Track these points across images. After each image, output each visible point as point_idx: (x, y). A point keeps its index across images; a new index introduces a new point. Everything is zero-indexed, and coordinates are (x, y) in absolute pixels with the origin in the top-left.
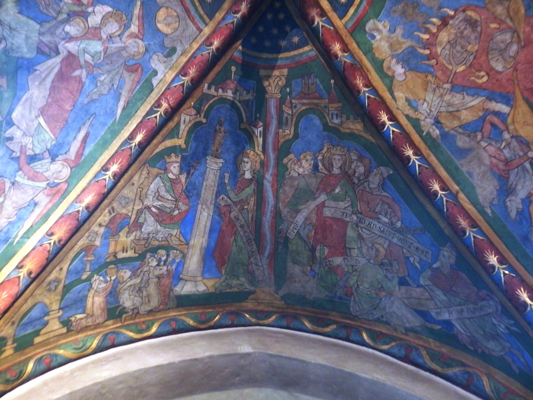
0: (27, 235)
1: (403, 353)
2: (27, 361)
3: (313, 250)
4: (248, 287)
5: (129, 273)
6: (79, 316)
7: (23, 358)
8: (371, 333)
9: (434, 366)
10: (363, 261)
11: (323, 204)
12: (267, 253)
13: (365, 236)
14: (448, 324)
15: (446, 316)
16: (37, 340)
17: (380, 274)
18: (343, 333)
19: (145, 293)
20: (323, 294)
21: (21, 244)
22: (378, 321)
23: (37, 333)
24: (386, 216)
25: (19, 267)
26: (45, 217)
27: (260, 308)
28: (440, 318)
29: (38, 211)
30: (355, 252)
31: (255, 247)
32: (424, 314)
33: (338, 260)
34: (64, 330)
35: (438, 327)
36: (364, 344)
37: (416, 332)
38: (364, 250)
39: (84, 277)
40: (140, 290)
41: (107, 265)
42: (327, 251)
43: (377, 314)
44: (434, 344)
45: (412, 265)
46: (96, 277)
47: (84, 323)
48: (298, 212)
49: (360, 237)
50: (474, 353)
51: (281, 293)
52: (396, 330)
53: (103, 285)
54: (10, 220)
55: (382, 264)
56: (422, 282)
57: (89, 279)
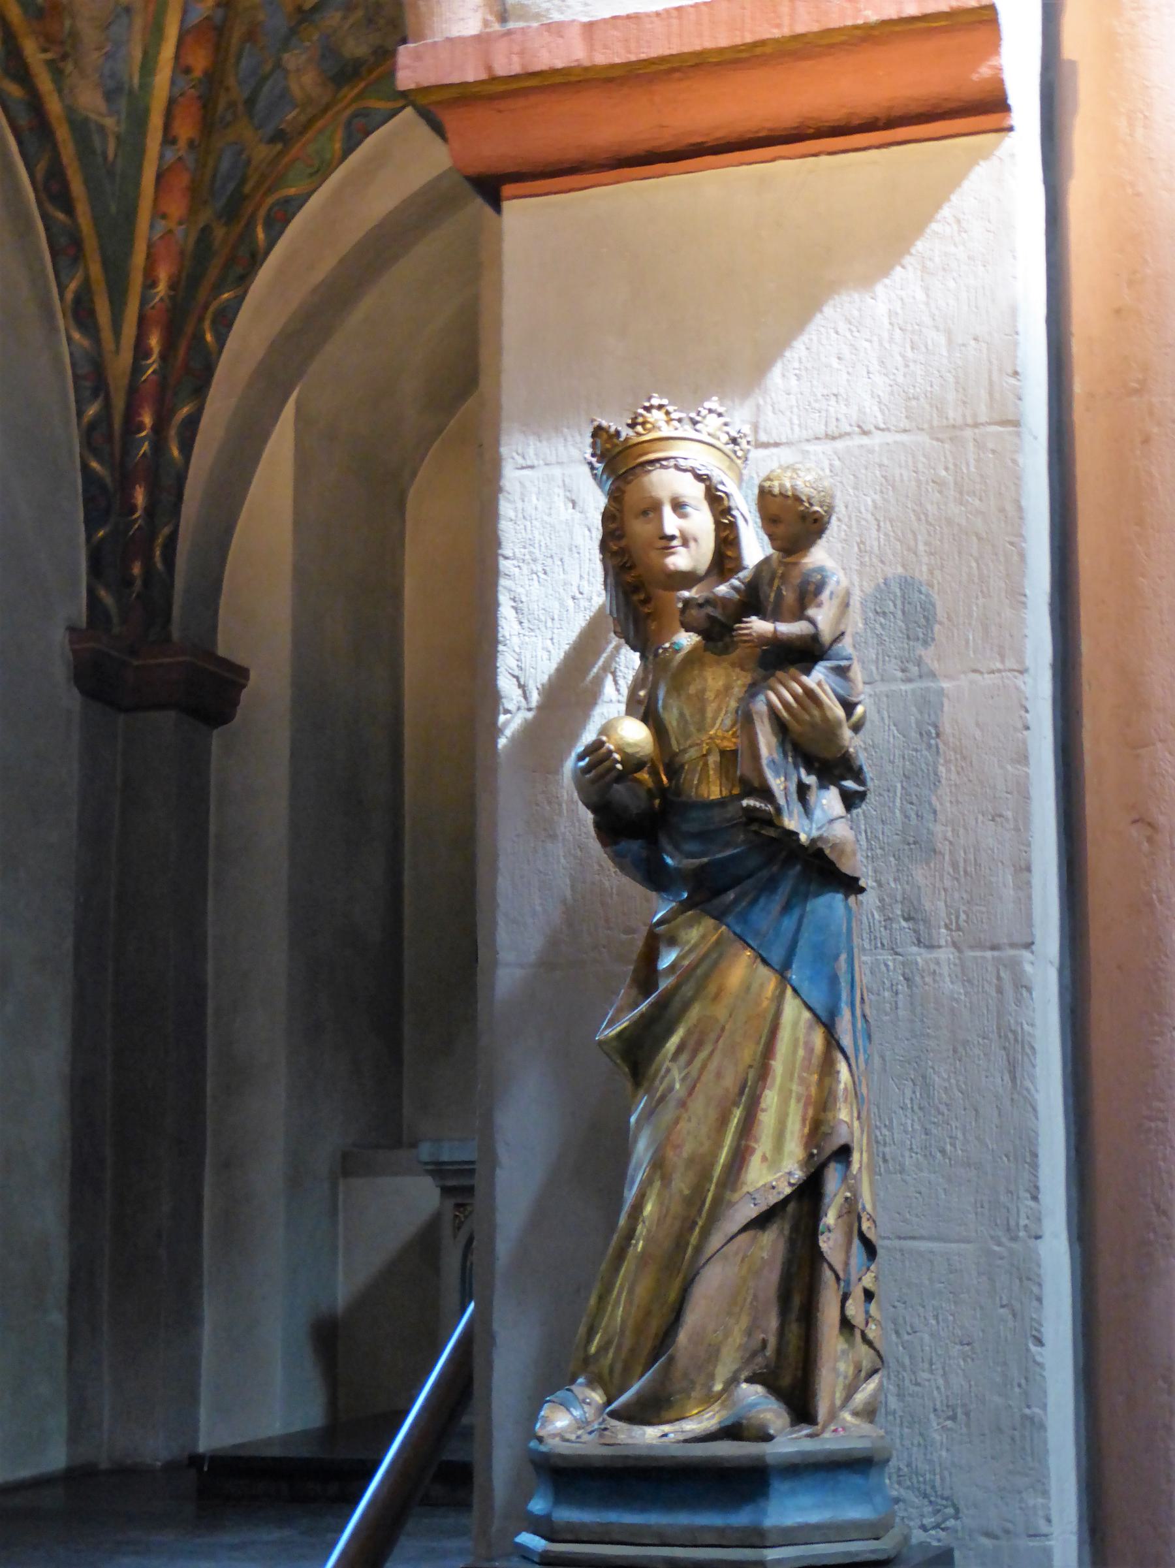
0: (148, 66)
2: (250, 225)
5: (338, 15)
6: (290, 117)
7: (242, 223)
16: (247, 189)
19: (382, 22)
21: (146, 86)
23: (243, 181)
25: (169, 139)
26: (156, 31)
29: (138, 22)
34: (279, 146)
39: (268, 67)
40: (370, 21)
41: (293, 31)
46: (286, 56)
47: (303, 118)
53: (304, 57)
54: (104, 51)
57: (278, 65)
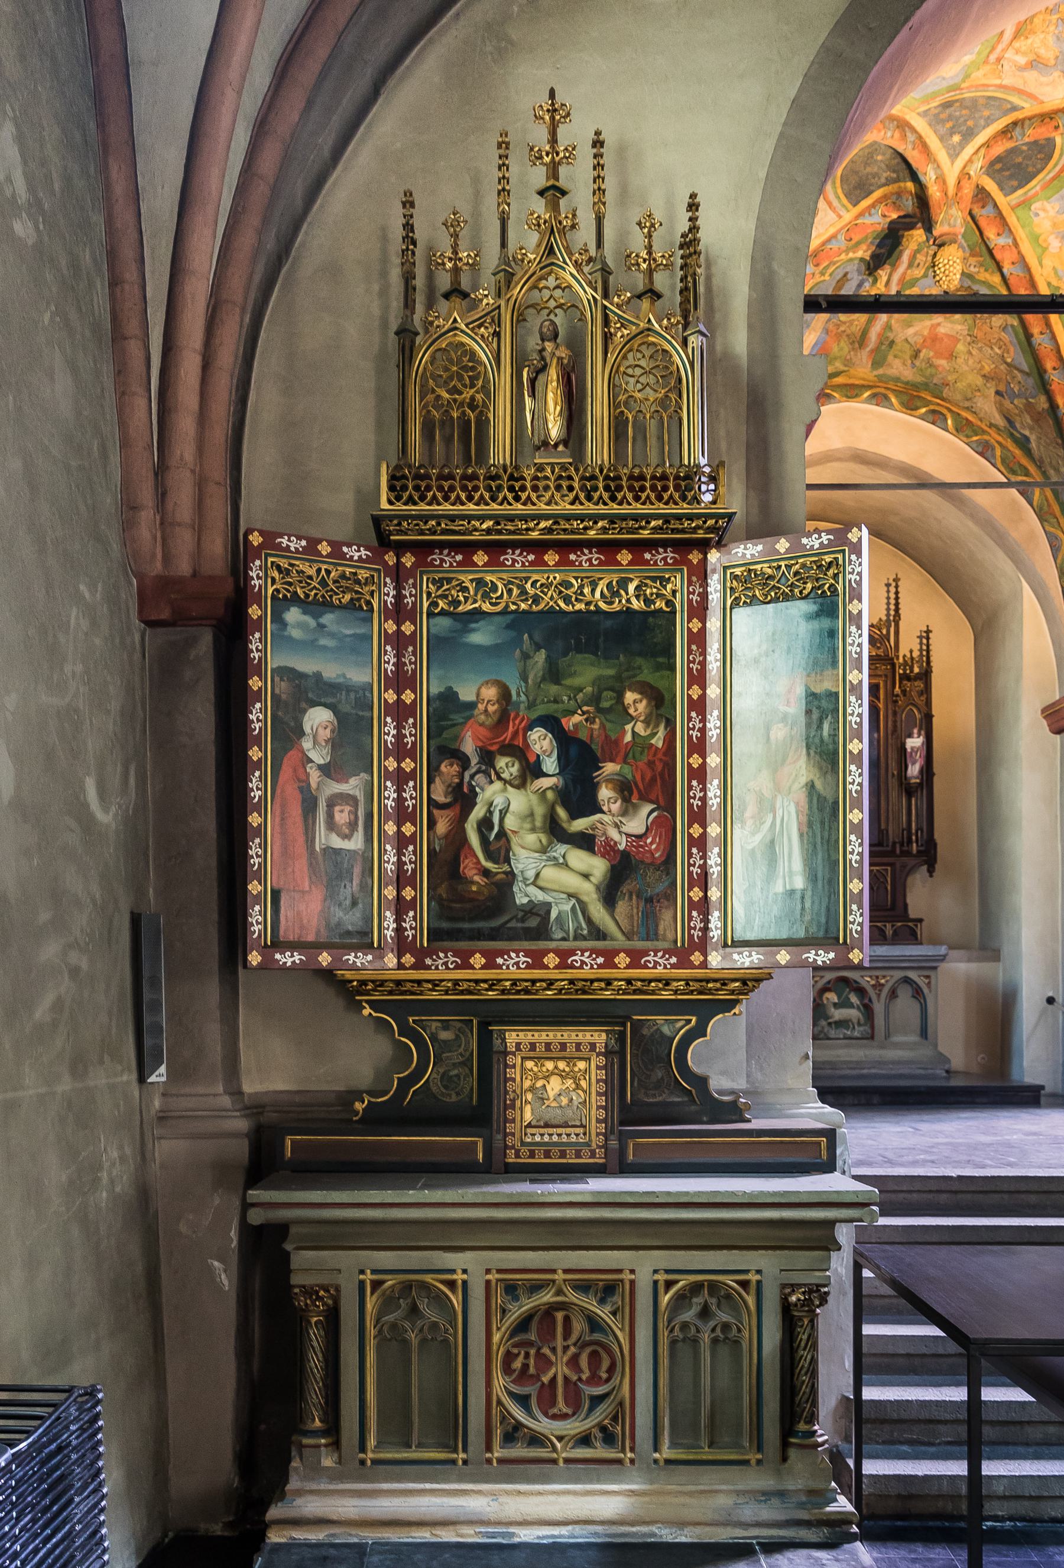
1: (980, 449)
3: (919, 351)
4: (842, 368)
8: (956, 416)
9: (1002, 469)
10: (966, 368)
11: (939, 324)
12: (868, 349)
13: (974, 352)
14: (1027, 439)
15: (1027, 433)
17: (979, 381)
18: (931, 417)
20: (919, 379)
22: (967, 409)
24: (1000, 348)
27: (851, 381)
28: (1022, 431)
30: (960, 361)
31: (857, 345)
32: (1010, 422)
33: (943, 362)
35: (1018, 435)
36: (947, 431)
37: (999, 429)
38: (971, 362)
42: (932, 354)
43: (967, 404)
44: (1010, 444)
45: (1012, 389)
48: (910, 326)
49: (970, 353)
50: (1039, 467)
51: (875, 373)
52: (981, 420)
55: (984, 376)
56: (1016, 402)
